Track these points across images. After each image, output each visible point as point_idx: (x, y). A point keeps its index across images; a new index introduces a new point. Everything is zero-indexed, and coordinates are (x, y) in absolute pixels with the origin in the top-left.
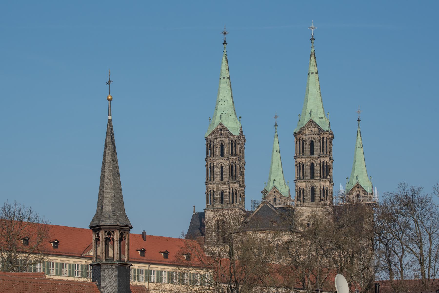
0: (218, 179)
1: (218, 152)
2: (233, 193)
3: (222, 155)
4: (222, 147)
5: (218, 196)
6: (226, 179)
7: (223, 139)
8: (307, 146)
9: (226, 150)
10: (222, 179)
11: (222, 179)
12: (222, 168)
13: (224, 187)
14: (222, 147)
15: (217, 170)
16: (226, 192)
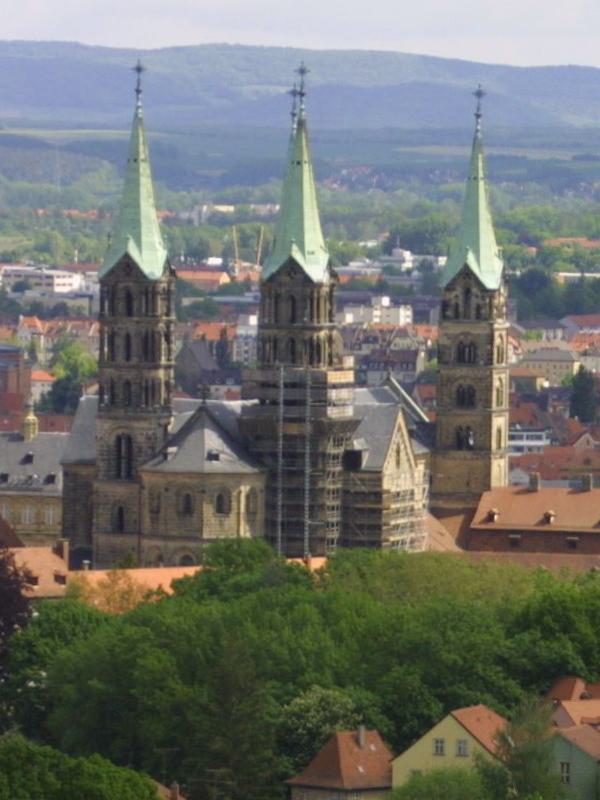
0: (120, 358)
1: (121, 306)
2: (147, 388)
3: (129, 312)
4: (129, 298)
5: (120, 391)
6: (134, 360)
7: (131, 284)
8: (285, 309)
9: (135, 305)
10: (128, 357)
11: (128, 357)
12: (128, 338)
13: (129, 375)
14: (129, 298)
15: (120, 342)
16: (135, 383)
